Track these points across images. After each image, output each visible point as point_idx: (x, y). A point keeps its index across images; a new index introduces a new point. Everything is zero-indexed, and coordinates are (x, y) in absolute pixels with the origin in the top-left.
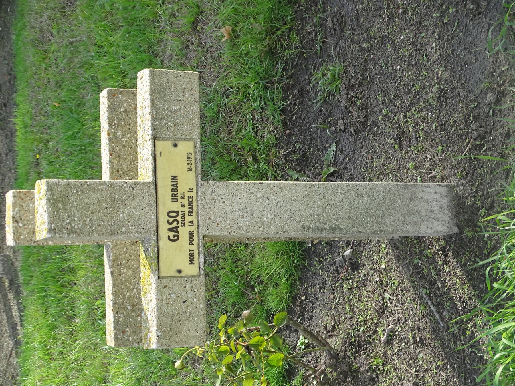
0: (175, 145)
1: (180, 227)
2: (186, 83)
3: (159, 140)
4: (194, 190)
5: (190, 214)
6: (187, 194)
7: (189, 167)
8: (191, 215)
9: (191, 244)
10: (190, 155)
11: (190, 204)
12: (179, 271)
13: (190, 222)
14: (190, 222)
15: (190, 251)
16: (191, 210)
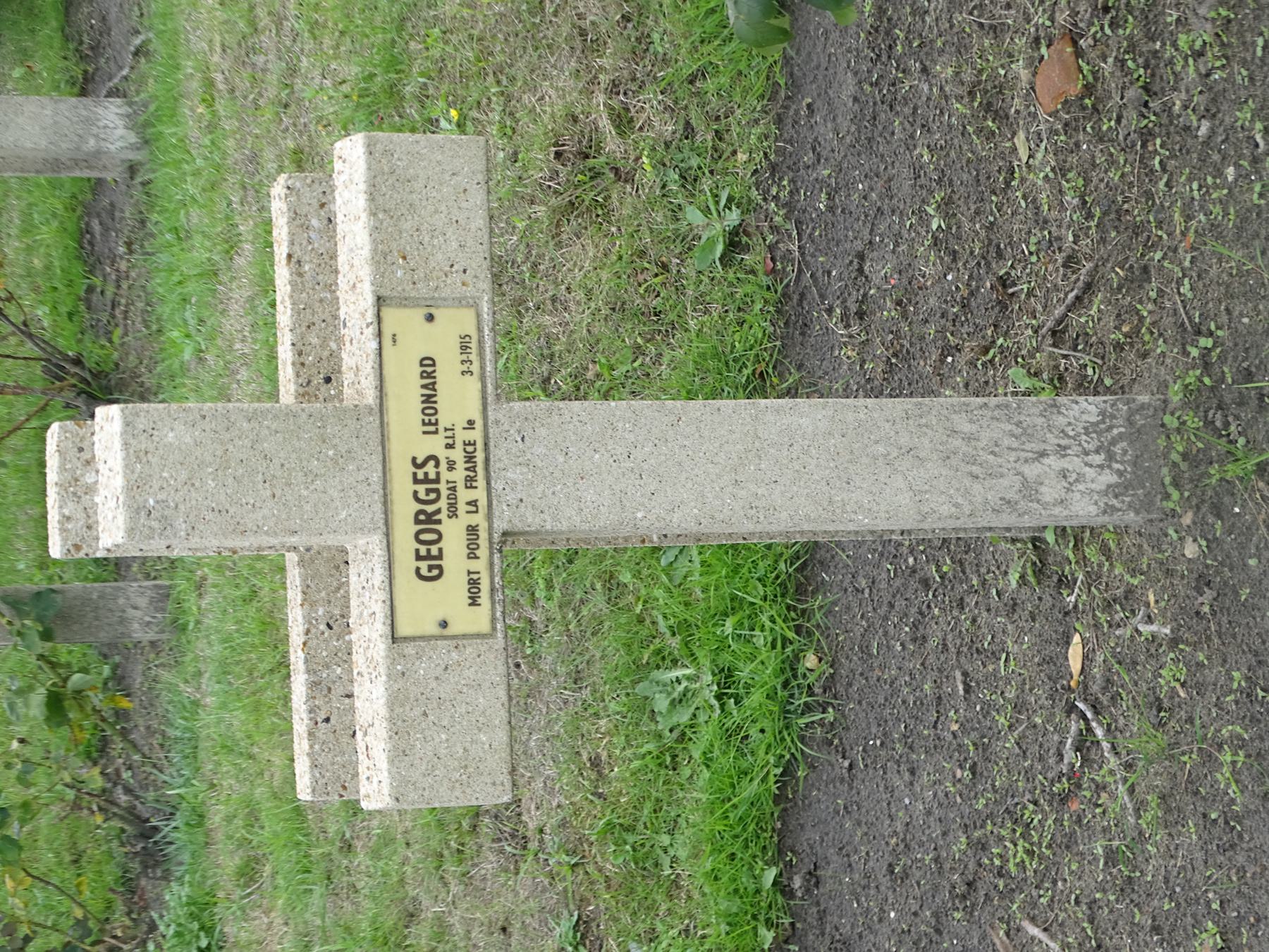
0: (430, 318)
1: (443, 516)
2: (454, 171)
3: (388, 305)
4: (479, 424)
5: (470, 482)
6: (461, 436)
7: (465, 368)
8: (471, 487)
9: (472, 556)
10: (467, 339)
11: (470, 458)
12: (444, 624)
13: (469, 503)
14: (469, 503)
15: (469, 573)
16: (472, 474)
